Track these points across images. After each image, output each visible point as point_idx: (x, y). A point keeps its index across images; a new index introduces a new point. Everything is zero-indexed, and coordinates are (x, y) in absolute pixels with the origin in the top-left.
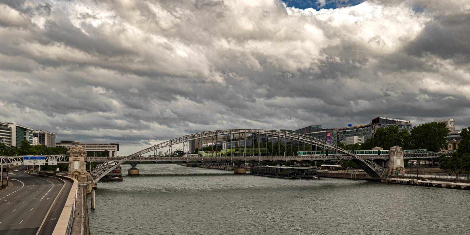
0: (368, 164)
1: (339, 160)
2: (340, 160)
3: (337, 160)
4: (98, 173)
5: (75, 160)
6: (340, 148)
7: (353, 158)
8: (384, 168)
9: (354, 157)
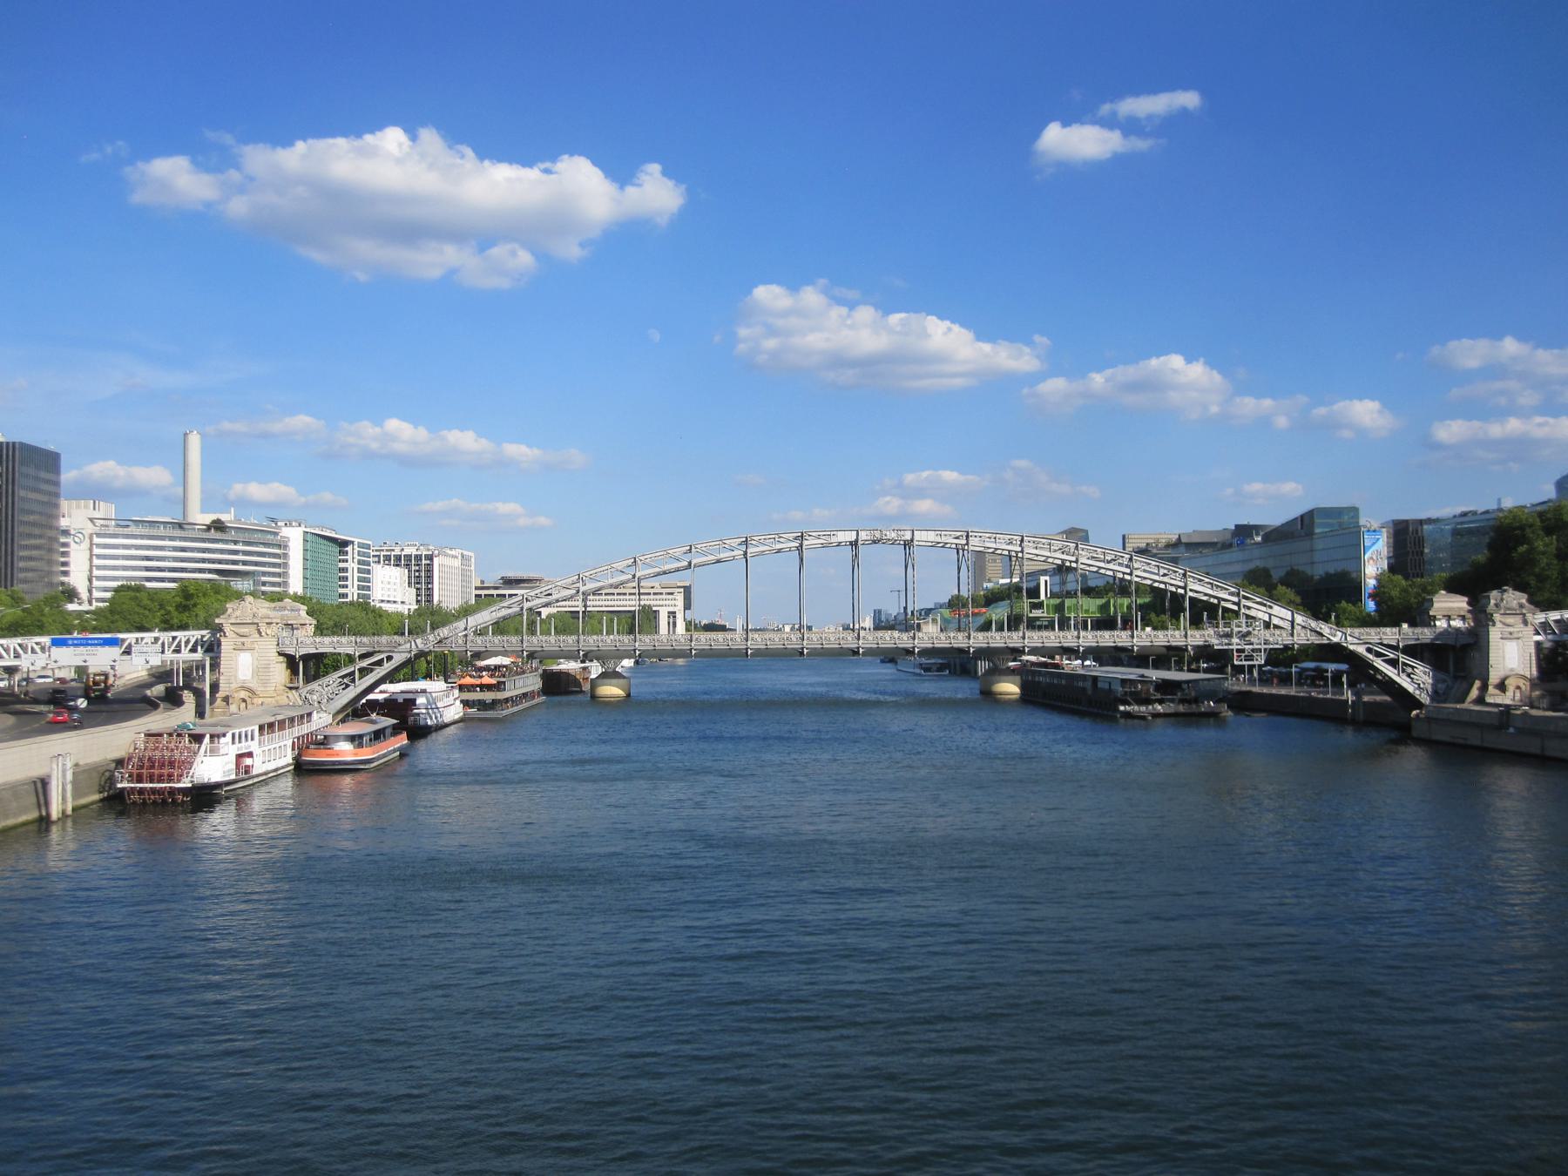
0: (1384, 661)
1: (1247, 647)
2: (1251, 647)
3: (1239, 647)
4: (324, 693)
5: (241, 648)
6: (1259, 600)
7: (1316, 640)
8: (1456, 678)
9: (1321, 635)
